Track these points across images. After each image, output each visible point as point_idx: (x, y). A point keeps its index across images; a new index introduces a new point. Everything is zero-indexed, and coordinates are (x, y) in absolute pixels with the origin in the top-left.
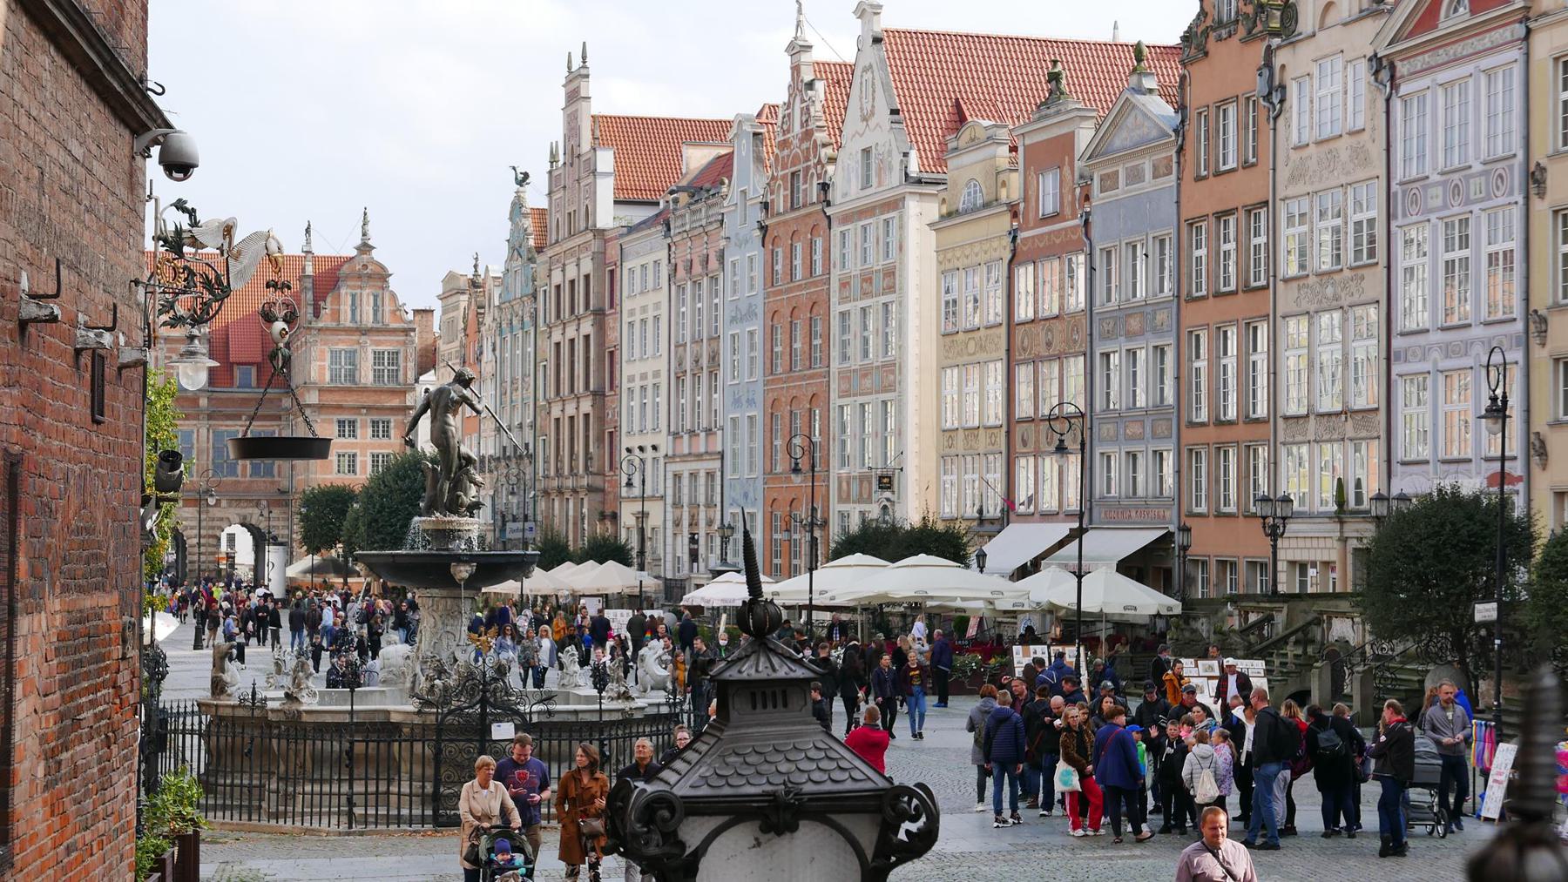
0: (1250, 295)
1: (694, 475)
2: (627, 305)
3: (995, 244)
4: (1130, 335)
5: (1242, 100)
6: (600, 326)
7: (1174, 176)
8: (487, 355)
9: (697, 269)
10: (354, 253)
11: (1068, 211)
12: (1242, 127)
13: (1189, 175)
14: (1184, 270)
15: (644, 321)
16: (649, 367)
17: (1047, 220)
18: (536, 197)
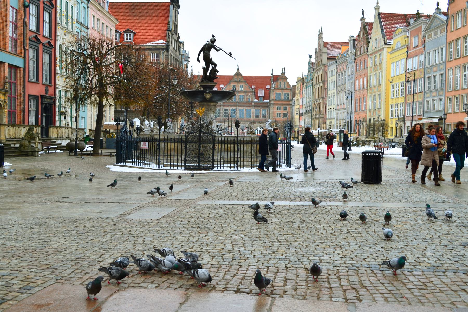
0: (464, 58)
1: (341, 113)
2: (329, 79)
3: (403, 55)
4: (434, 72)
5: (463, 10)
6: (324, 84)
7: (445, 32)
8: (304, 93)
9: (342, 70)
10: (281, 75)
11: (420, 45)
12: (463, 17)
13: (449, 31)
14: (447, 54)
15: (332, 82)
16: (332, 92)
17: (415, 47)
18: (313, 60)
